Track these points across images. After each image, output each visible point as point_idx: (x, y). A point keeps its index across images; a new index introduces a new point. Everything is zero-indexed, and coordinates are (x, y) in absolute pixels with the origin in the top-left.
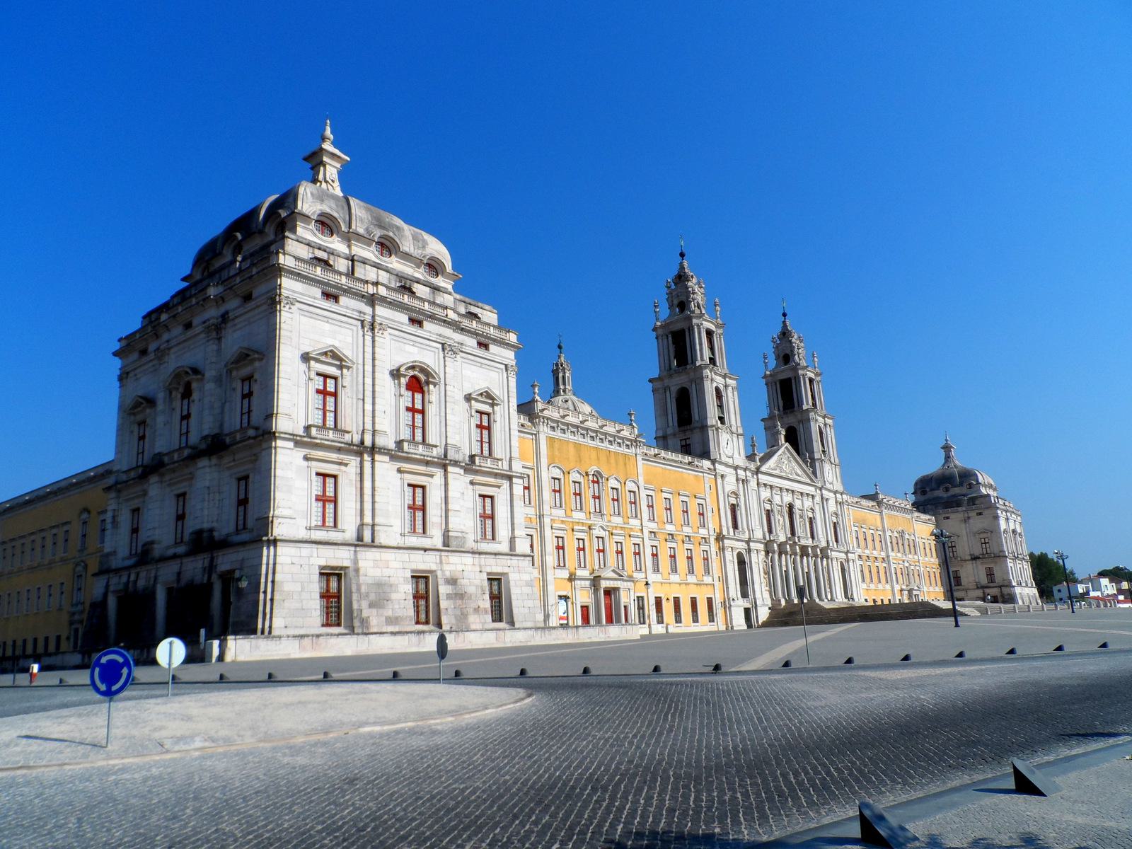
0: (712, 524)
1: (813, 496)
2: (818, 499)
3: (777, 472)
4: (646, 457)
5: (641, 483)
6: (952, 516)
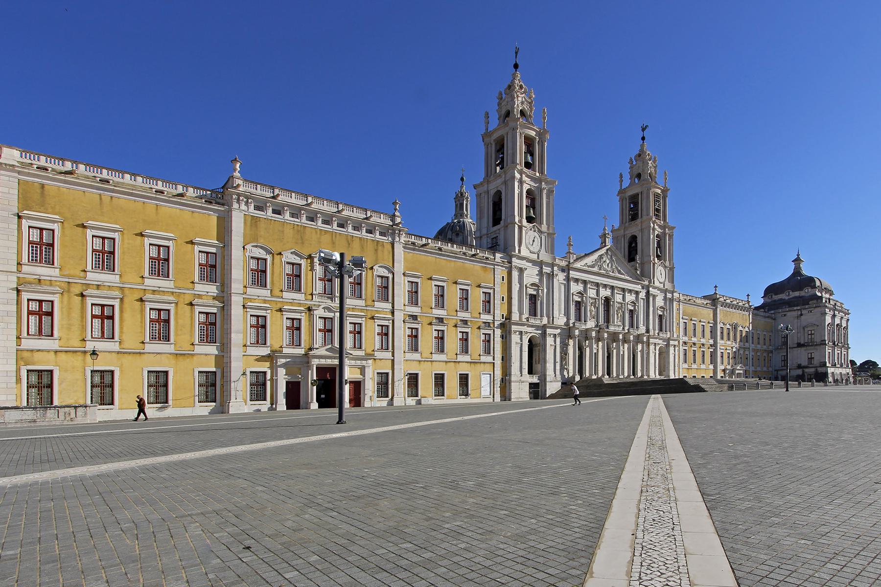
0: (499, 311)
1: (637, 293)
2: (642, 295)
3: (596, 269)
4: (411, 247)
5: (399, 268)
6: (789, 314)
